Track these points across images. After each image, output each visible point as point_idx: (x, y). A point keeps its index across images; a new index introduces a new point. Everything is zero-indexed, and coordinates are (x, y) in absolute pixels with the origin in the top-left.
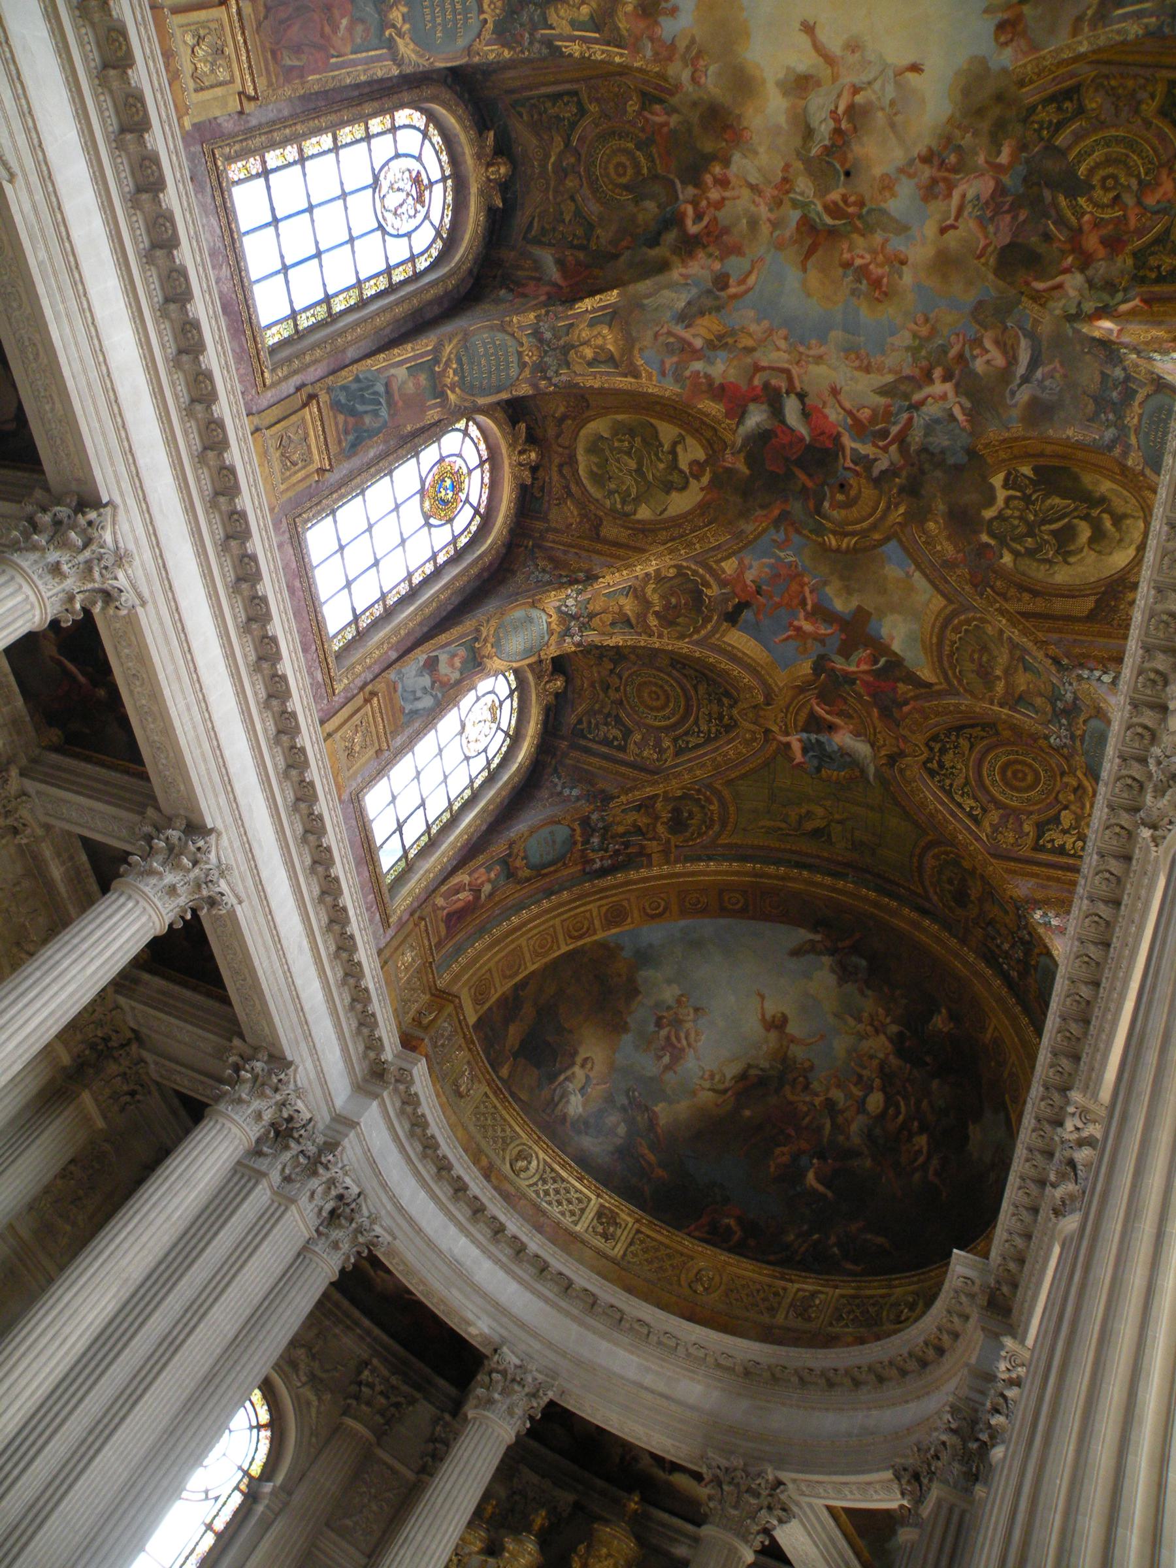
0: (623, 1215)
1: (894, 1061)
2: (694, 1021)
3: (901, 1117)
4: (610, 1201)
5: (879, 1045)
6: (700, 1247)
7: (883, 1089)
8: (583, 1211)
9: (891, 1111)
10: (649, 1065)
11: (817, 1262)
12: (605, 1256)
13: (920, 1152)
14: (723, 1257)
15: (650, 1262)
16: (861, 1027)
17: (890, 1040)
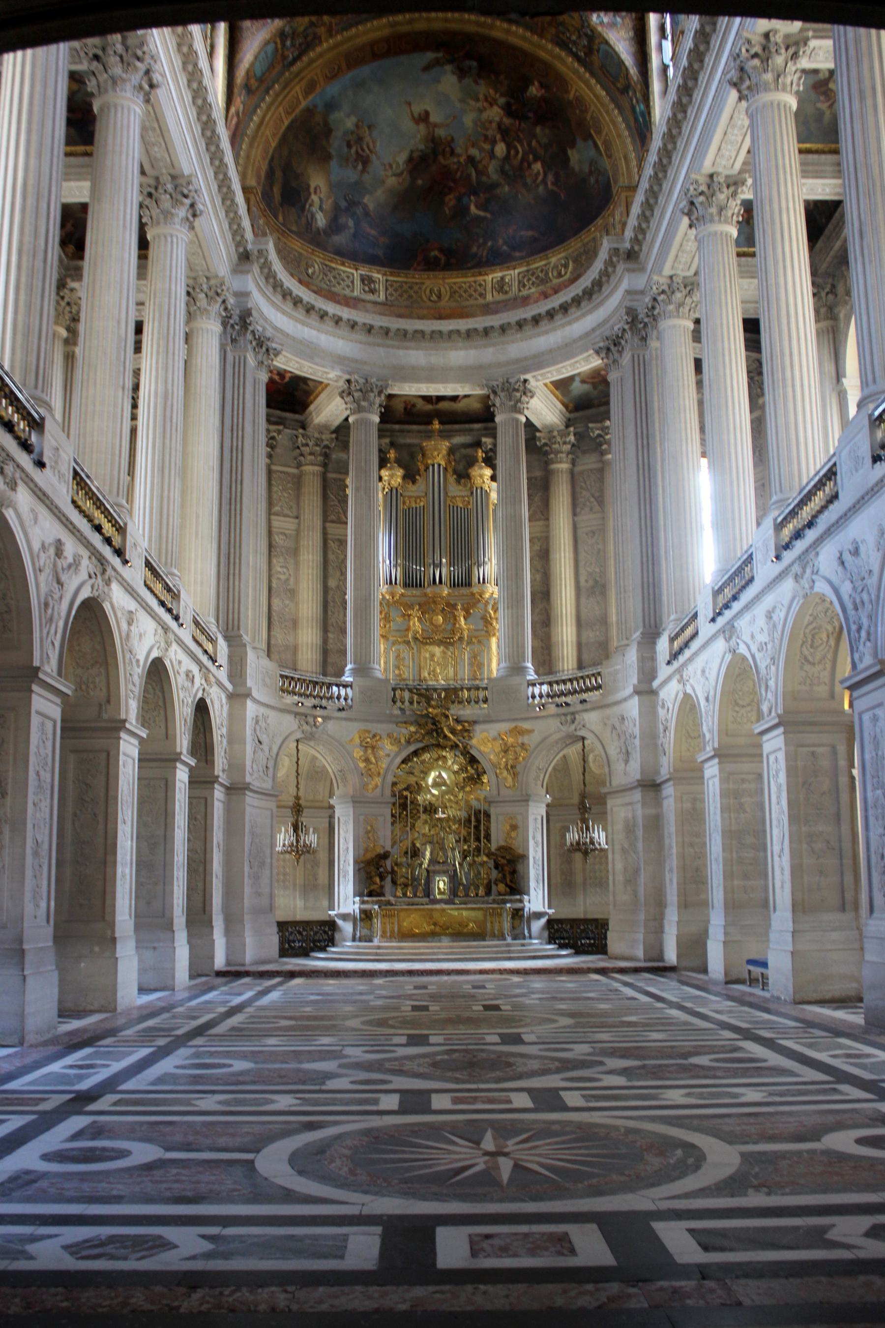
0: (376, 276)
1: (507, 121)
2: (370, 135)
3: (520, 155)
4: (363, 271)
5: (495, 113)
6: (425, 275)
7: (503, 140)
8: (353, 282)
9: (512, 152)
10: (351, 175)
11: (497, 259)
12: (375, 303)
13: (538, 173)
14: (441, 274)
15: (401, 296)
16: (479, 105)
17: (502, 108)
